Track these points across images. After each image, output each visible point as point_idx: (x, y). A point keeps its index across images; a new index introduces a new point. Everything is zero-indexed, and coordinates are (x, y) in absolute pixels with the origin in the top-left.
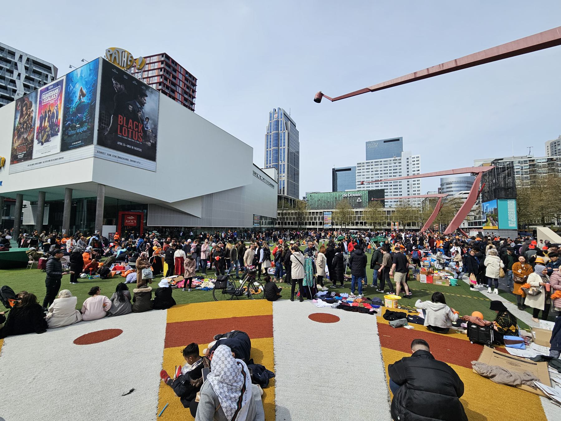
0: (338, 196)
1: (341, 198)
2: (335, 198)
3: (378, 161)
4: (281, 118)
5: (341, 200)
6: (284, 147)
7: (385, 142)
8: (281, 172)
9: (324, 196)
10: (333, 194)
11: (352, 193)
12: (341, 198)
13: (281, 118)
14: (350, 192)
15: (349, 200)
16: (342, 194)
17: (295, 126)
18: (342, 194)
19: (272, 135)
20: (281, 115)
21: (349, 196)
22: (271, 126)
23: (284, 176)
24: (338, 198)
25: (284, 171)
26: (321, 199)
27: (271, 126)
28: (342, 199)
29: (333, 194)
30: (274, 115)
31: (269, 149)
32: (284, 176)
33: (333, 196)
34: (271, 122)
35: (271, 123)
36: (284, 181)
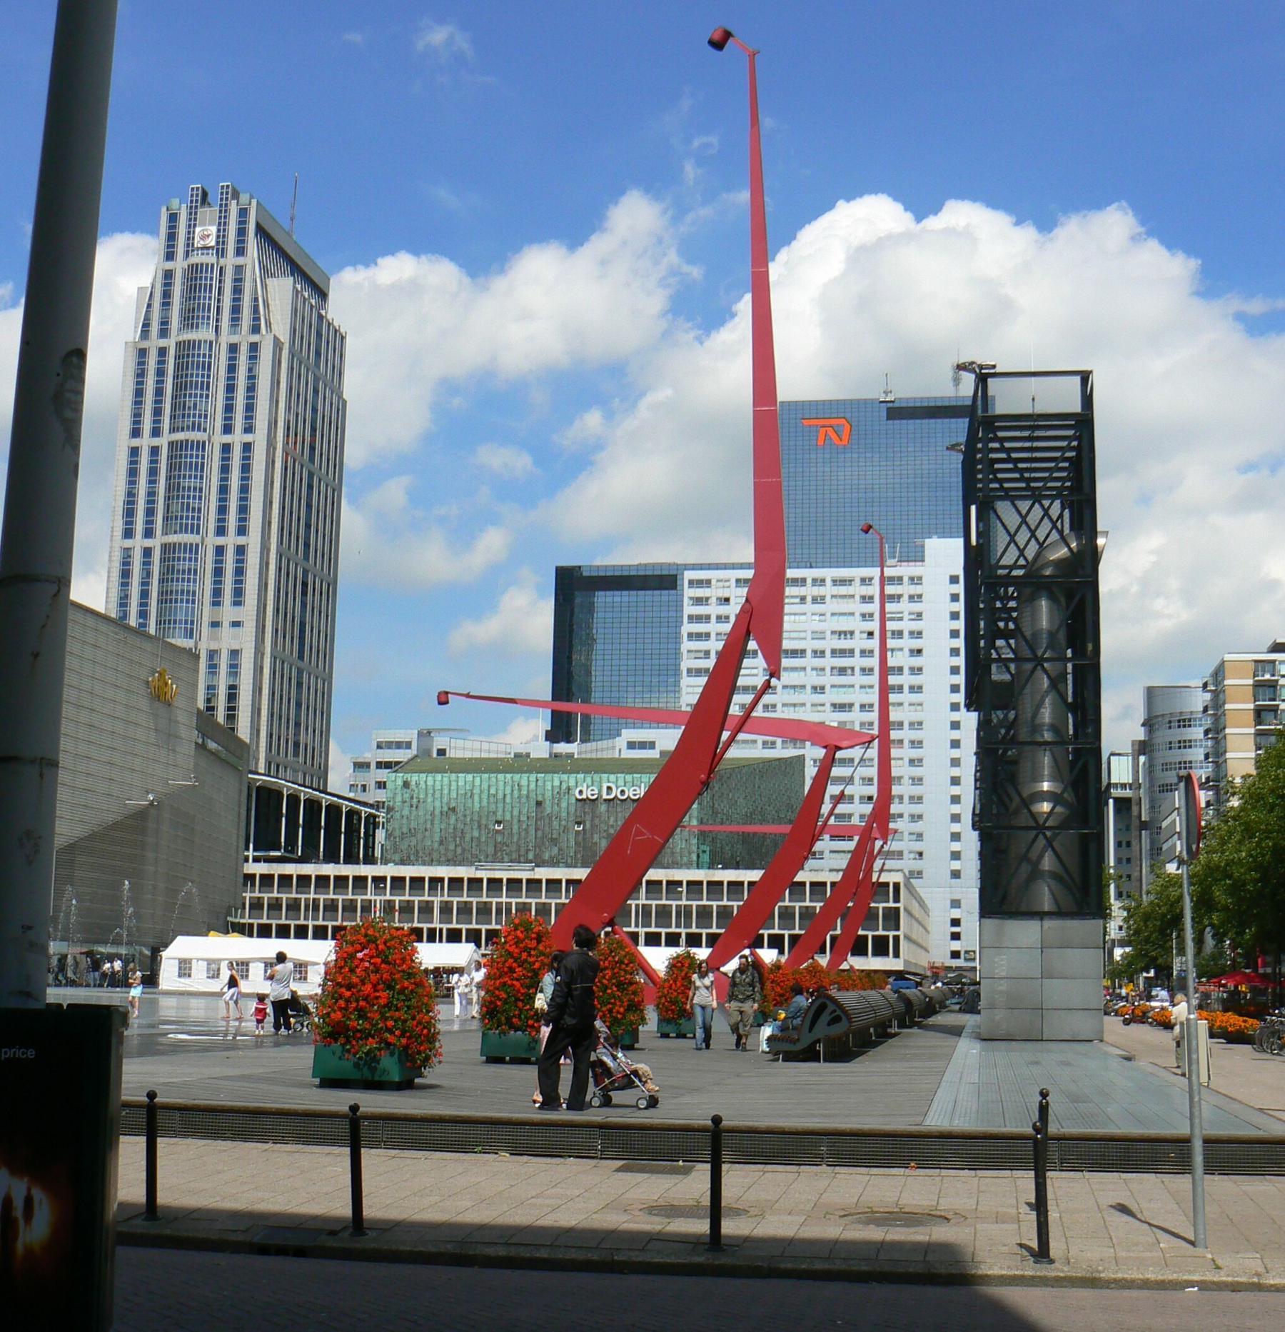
0: (548, 794)
1: (564, 805)
2: (533, 803)
3: (804, 580)
4: (240, 251)
5: (564, 814)
6: (248, 438)
7: (898, 412)
8: (217, 593)
9: (477, 791)
10: (524, 782)
11: (621, 782)
12: (564, 805)
13: (240, 251)
14: (612, 777)
15: (605, 817)
16: (572, 783)
17: (323, 295)
18: (572, 783)
19: (172, 352)
20: (242, 232)
21: (605, 797)
22: (167, 294)
23: (236, 624)
24: (548, 803)
25: (238, 593)
26: (460, 809)
27: (167, 294)
28: (572, 809)
29: (524, 782)
30: (191, 227)
31: (146, 442)
32: (236, 624)
33: (524, 792)
34: (169, 265)
35: (168, 275)
36: (235, 654)
